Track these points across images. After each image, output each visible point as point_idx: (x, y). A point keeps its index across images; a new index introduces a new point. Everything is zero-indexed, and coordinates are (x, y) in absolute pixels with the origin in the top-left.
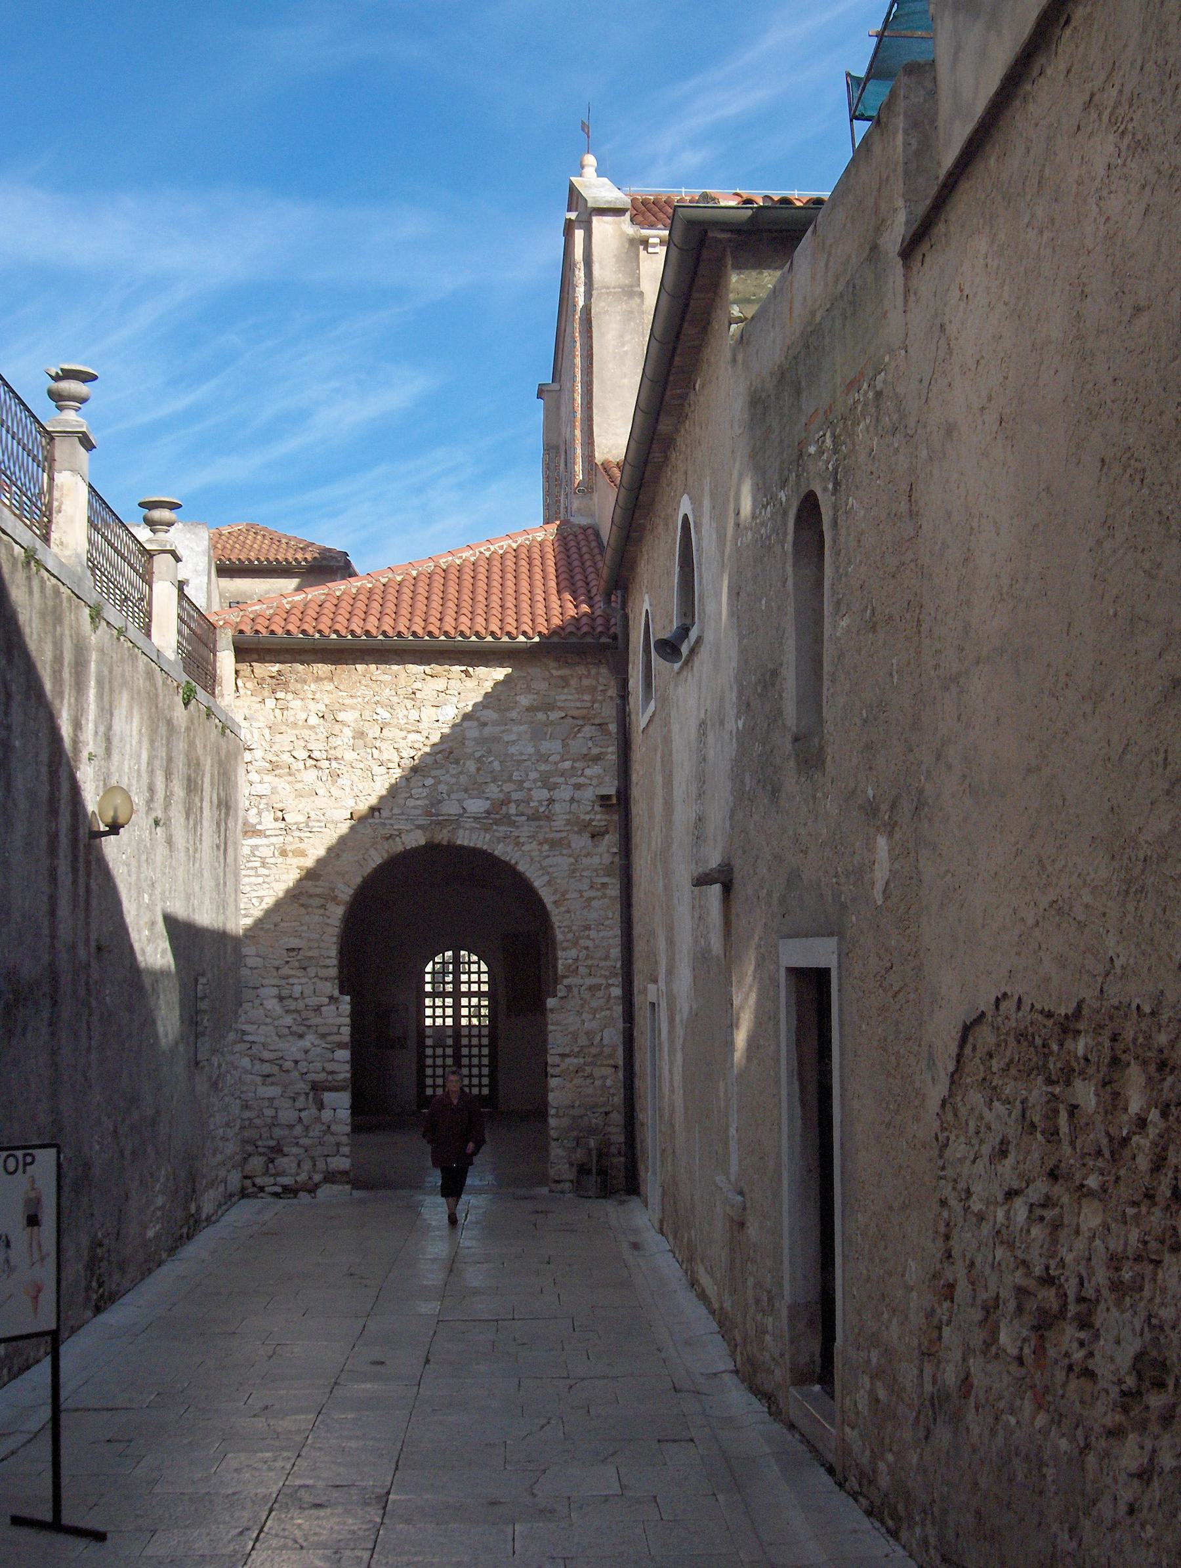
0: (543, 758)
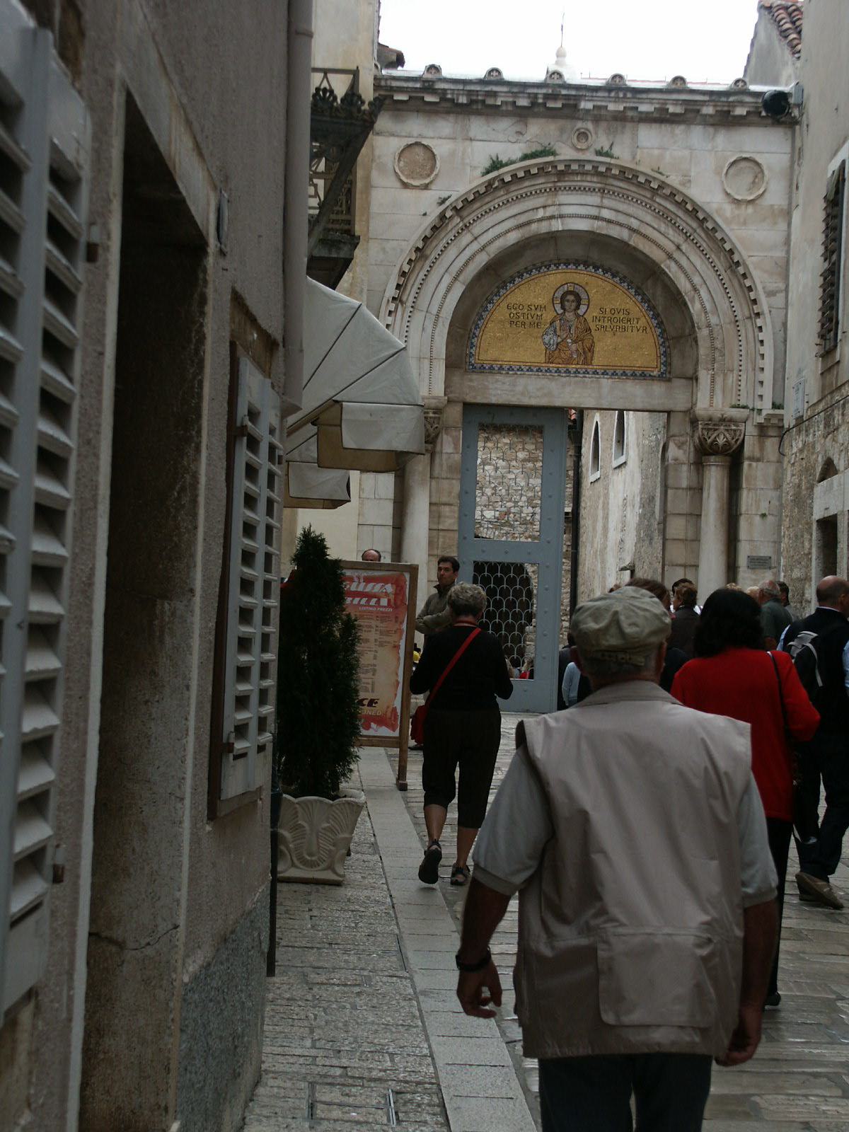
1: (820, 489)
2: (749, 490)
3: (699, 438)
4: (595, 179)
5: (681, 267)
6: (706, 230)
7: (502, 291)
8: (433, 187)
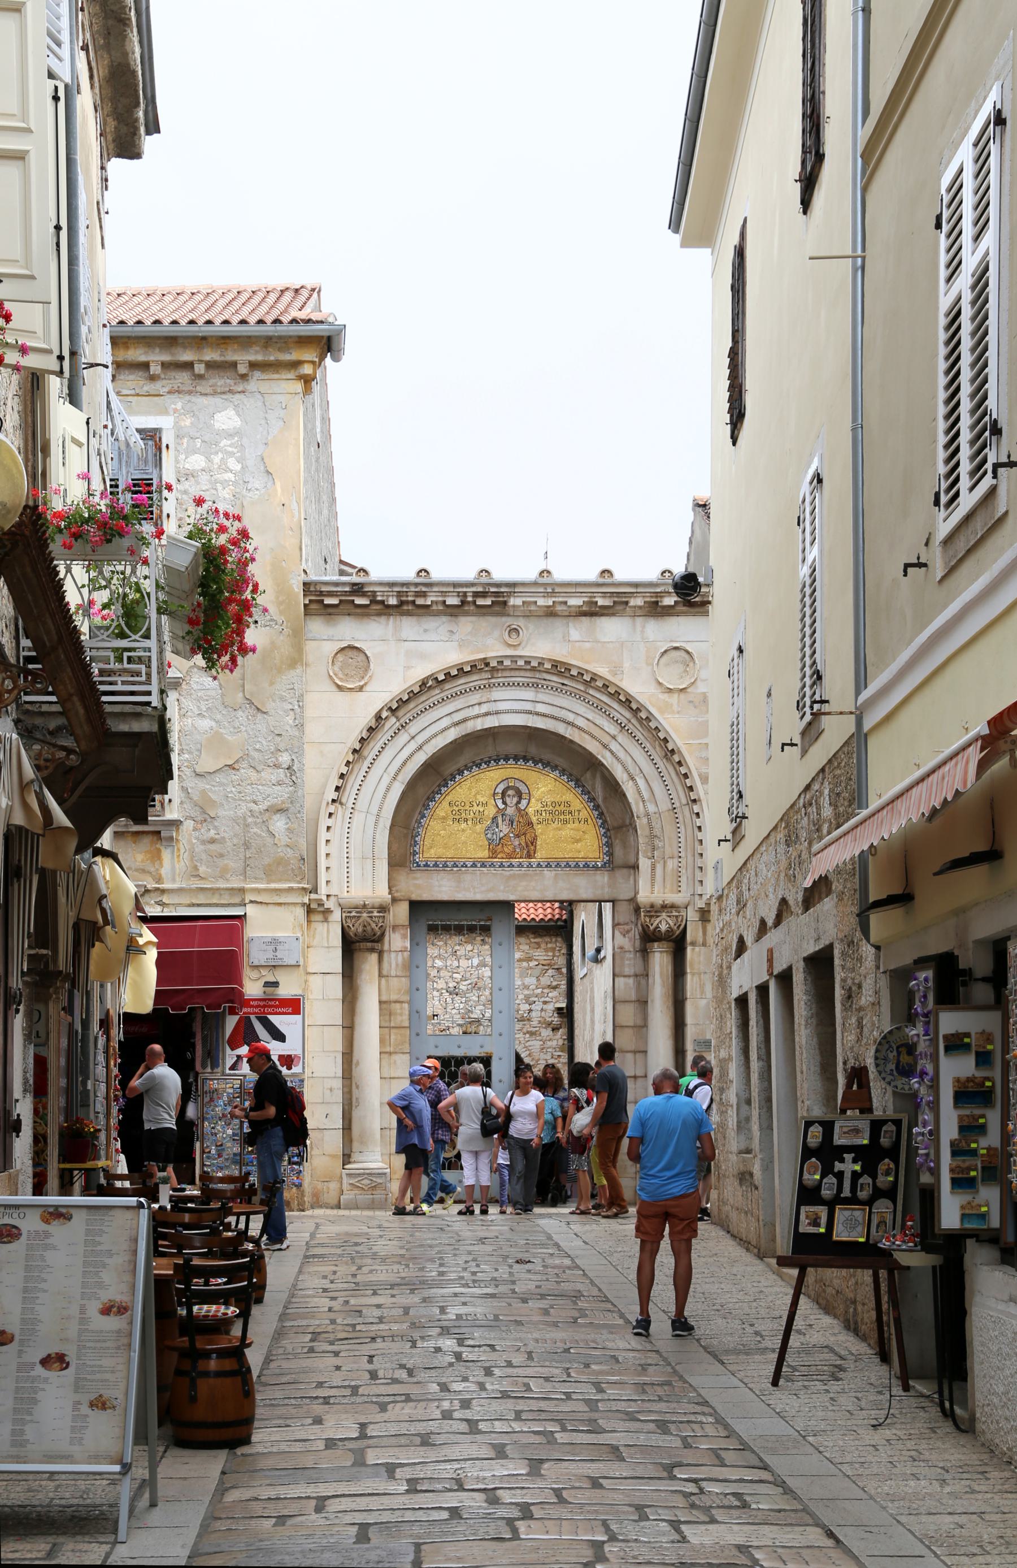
0: (527, 987)
1: (736, 965)
2: (693, 974)
3: (642, 925)
4: (528, 674)
5: (617, 758)
6: (640, 720)
7: (443, 790)
8: (367, 688)
